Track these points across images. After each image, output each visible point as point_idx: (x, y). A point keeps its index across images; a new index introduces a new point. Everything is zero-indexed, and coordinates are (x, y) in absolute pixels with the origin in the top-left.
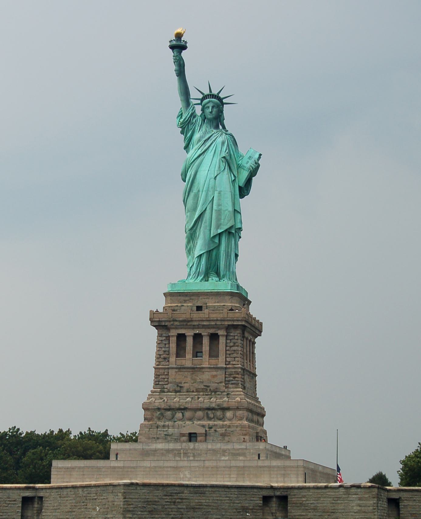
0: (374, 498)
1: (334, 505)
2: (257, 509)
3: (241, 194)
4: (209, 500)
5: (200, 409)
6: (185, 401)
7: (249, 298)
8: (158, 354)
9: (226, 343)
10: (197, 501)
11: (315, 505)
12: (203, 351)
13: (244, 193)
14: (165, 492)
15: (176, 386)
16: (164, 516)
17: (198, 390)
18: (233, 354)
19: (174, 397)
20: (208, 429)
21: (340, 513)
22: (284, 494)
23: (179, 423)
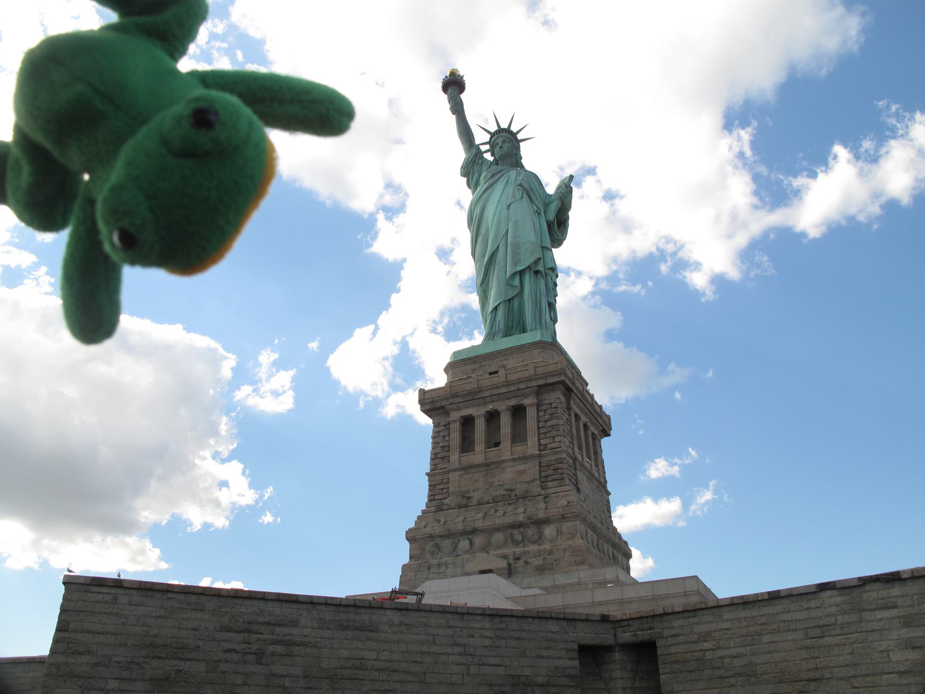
3: (554, 240)
5: (498, 529)
6: (474, 519)
9: (538, 416)
10: (344, 653)
13: (558, 237)
18: (550, 432)
19: (457, 515)
20: (513, 562)
23: (464, 557)
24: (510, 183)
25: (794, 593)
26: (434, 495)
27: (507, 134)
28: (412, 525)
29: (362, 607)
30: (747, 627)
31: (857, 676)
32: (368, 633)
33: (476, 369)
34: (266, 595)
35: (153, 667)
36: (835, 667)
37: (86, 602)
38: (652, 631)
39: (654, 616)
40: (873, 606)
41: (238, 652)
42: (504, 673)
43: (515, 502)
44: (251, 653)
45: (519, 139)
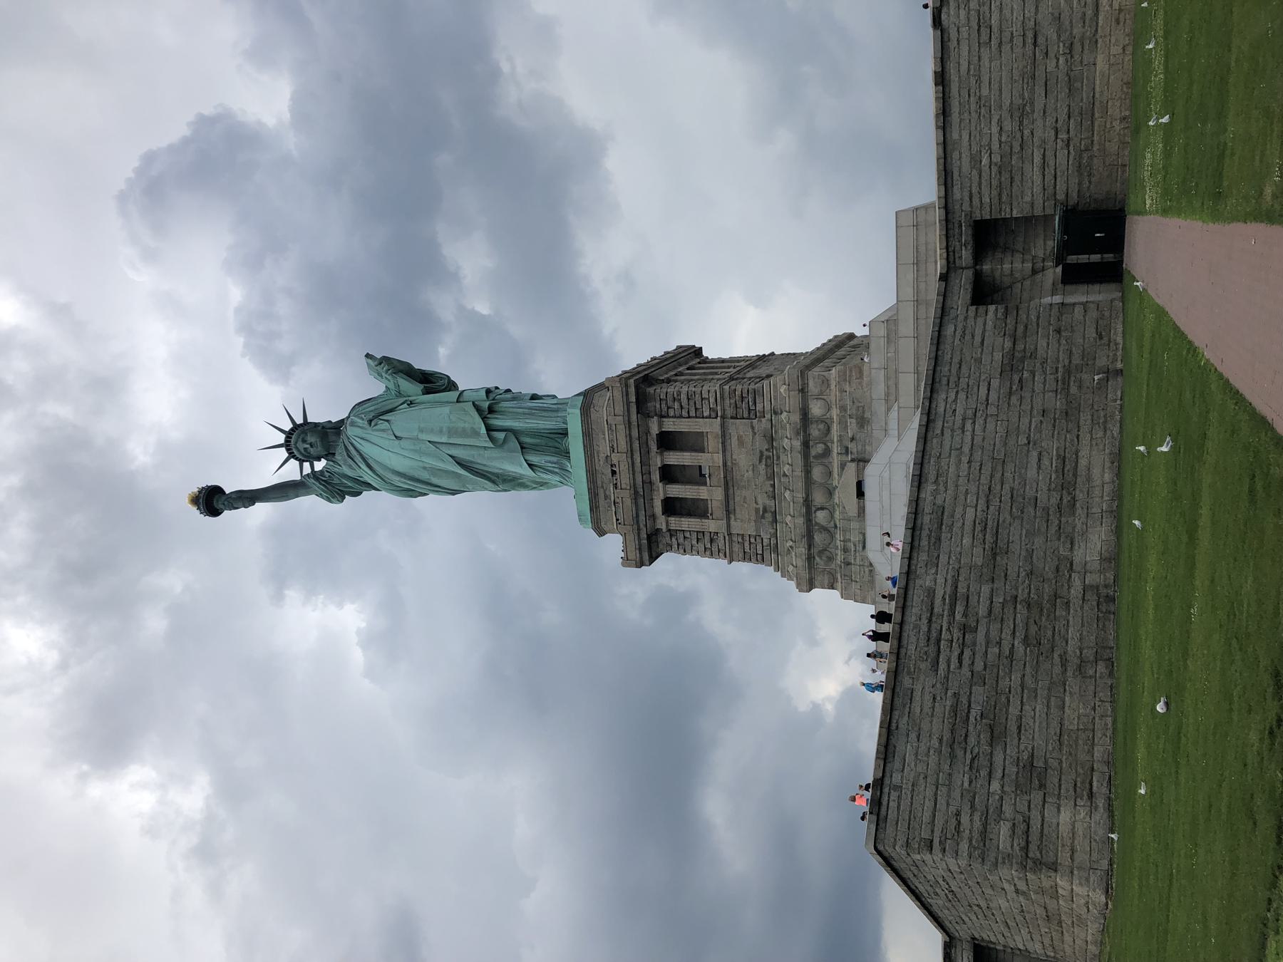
1: (1007, 35)
4: (967, 492)
5: (807, 471)
6: (792, 503)
8: (703, 553)
9: (675, 417)
10: (967, 541)
11: (1006, 115)
12: (698, 464)
14: (923, 666)
17: (769, 476)
18: (695, 403)
19: (784, 525)
22: (966, 234)
23: (838, 518)
24: (364, 436)
25: (940, 55)
26: (757, 554)
27: (293, 436)
29: (915, 523)
33: (605, 494)
34: (897, 622)
35: (976, 743)
37: (898, 820)
38: (963, 224)
39: (947, 220)
41: (962, 652)
42: (998, 380)
43: (777, 453)
44: (964, 638)
45: (302, 422)
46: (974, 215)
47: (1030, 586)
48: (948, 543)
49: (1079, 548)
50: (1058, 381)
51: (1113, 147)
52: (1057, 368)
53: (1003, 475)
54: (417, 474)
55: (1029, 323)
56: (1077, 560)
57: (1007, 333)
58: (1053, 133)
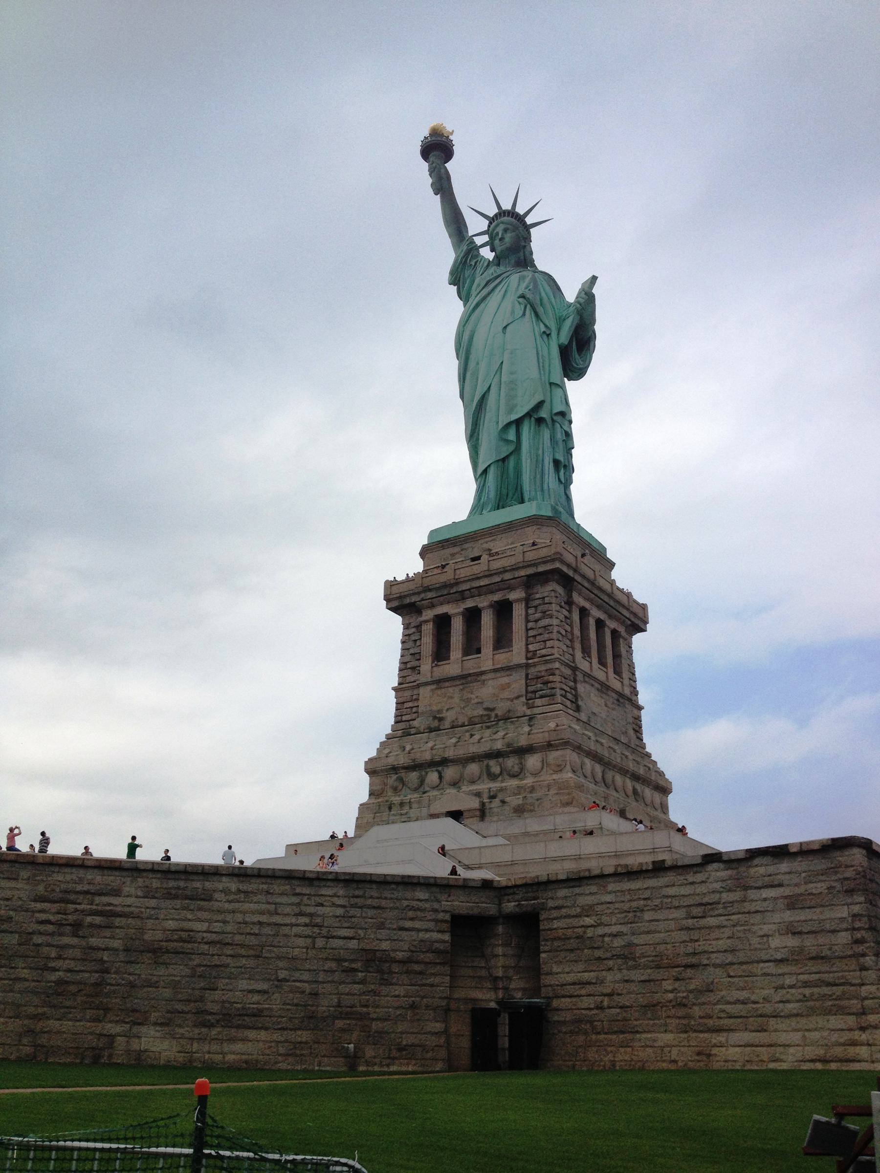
0: (850, 892)
1: (695, 935)
2: (427, 960)
4: (225, 922)
5: (473, 759)
6: (444, 746)
7: (610, 555)
9: (527, 615)
10: (171, 924)
13: (577, 365)
14: (41, 888)
15: (431, 718)
16: (25, 973)
18: (540, 634)
21: (715, 966)
24: (509, 293)
26: (402, 716)
28: (374, 754)
30: (630, 901)
31: (734, 964)
32: (199, 902)
36: (713, 952)
40: (759, 884)
42: (356, 947)
43: (493, 726)
44: (67, 925)
46: (543, 912)
47: (118, 985)
48: (170, 907)
49: (157, 1031)
50: (351, 1007)
51: (592, 1054)
52: (366, 1006)
53: (244, 956)
54: (473, 357)
55: (425, 977)
56: (144, 1029)
57: (414, 954)
58: (608, 991)
